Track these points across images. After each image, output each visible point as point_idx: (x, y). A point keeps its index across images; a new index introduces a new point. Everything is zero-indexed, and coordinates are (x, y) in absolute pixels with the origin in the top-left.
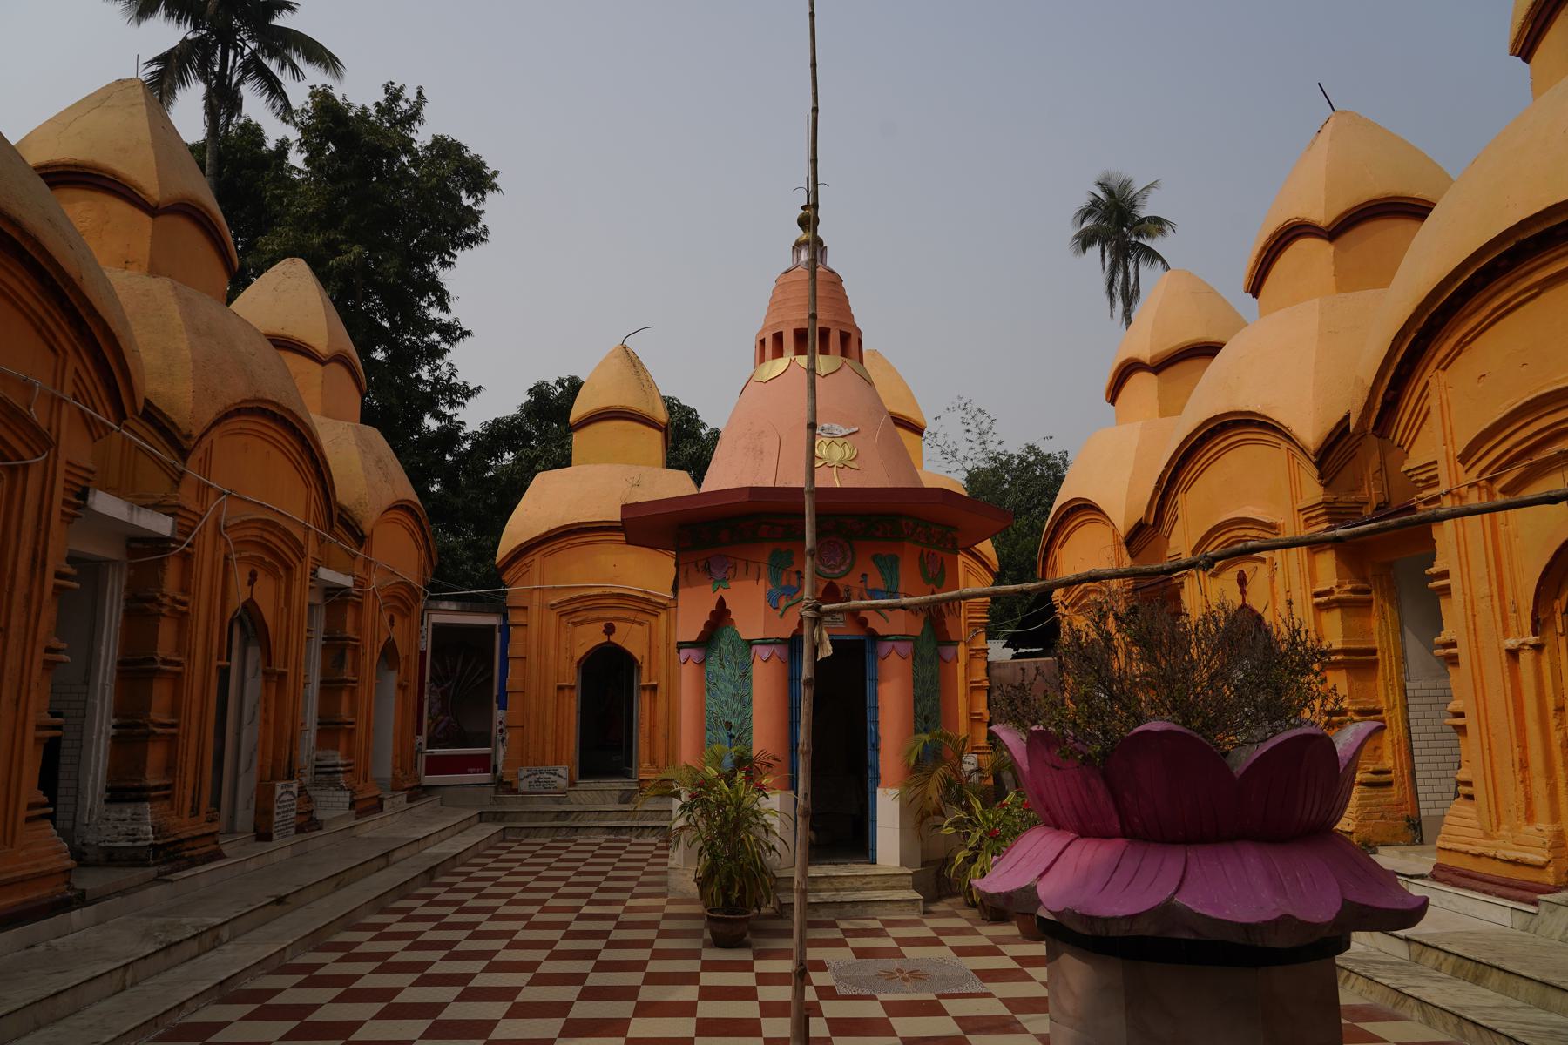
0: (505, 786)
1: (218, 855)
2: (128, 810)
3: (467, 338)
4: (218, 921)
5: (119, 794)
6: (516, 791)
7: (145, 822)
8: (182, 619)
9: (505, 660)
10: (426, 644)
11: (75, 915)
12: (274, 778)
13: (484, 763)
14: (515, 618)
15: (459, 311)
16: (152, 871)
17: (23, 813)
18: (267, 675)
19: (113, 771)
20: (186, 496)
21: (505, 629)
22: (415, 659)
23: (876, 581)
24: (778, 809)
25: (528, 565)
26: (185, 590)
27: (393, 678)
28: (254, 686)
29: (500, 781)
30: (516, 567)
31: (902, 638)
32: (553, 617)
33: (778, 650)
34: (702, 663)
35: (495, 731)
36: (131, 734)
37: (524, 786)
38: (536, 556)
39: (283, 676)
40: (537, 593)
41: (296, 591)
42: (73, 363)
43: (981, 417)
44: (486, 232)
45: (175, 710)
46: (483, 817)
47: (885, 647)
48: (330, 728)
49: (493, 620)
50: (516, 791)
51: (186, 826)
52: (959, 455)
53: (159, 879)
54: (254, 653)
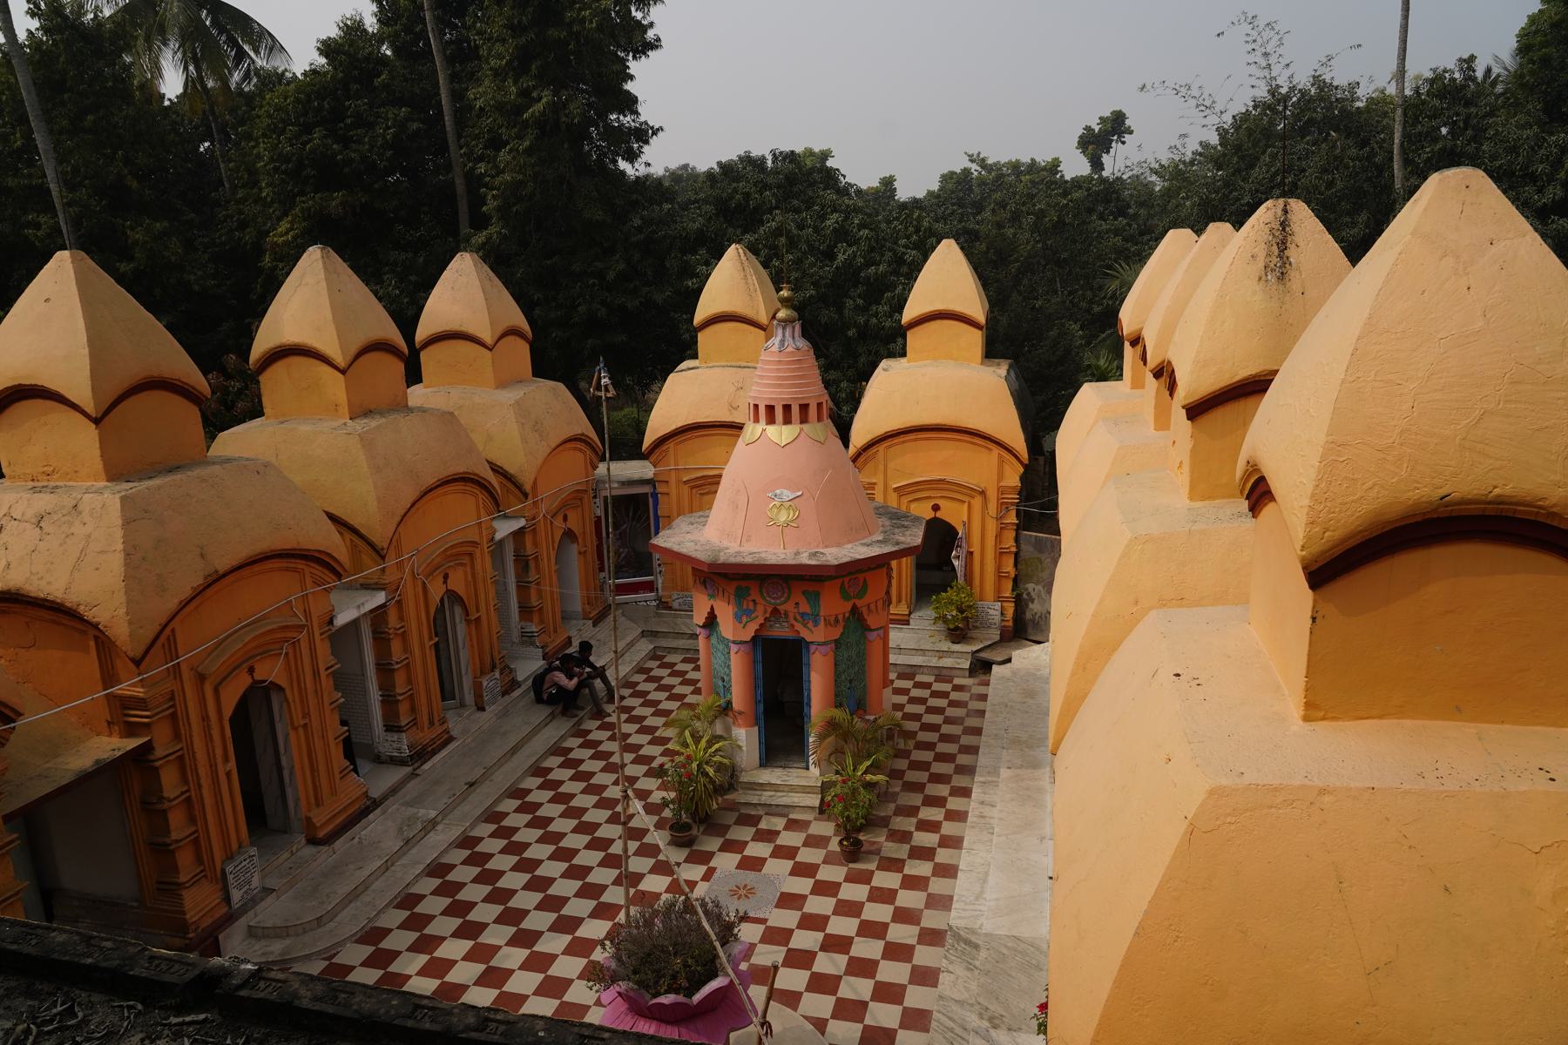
0: (664, 605)
1: (451, 739)
2: (396, 736)
3: (660, 134)
4: (433, 814)
5: (390, 728)
6: (670, 608)
7: (402, 744)
8: (404, 636)
9: (657, 518)
10: (600, 512)
11: (371, 816)
12: (483, 673)
13: (649, 586)
14: (659, 490)
15: (648, 113)
16: (409, 769)
17: (338, 776)
18: (468, 622)
19: (385, 717)
20: (389, 578)
21: (655, 495)
22: (590, 528)
23: (805, 607)
24: (745, 738)
25: (667, 451)
26: (401, 619)
27: (574, 549)
28: (461, 628)
29: (659, 599)
30: (657, 452)
31: (824, 644)
32: (686, 489)
33: (743, 647)
34: (708, 638)
35: (656, 563)
36: (389, 702)
37: (675, 605)
38: (671, 445)
39: (478, 620)
40: (673, 474)
41: (478, 567)
42: (307, 570)
43: (1267, 34)
44: (658, 40)
45: (409, 682)
46: (643, 634)
47: (813, 648)
48: (526, 611)
49: (646, 489)
50: (670, 608)
51: (426, 736)
52: (1218, 107)
53: (414, 775)
54: (458, 610)
